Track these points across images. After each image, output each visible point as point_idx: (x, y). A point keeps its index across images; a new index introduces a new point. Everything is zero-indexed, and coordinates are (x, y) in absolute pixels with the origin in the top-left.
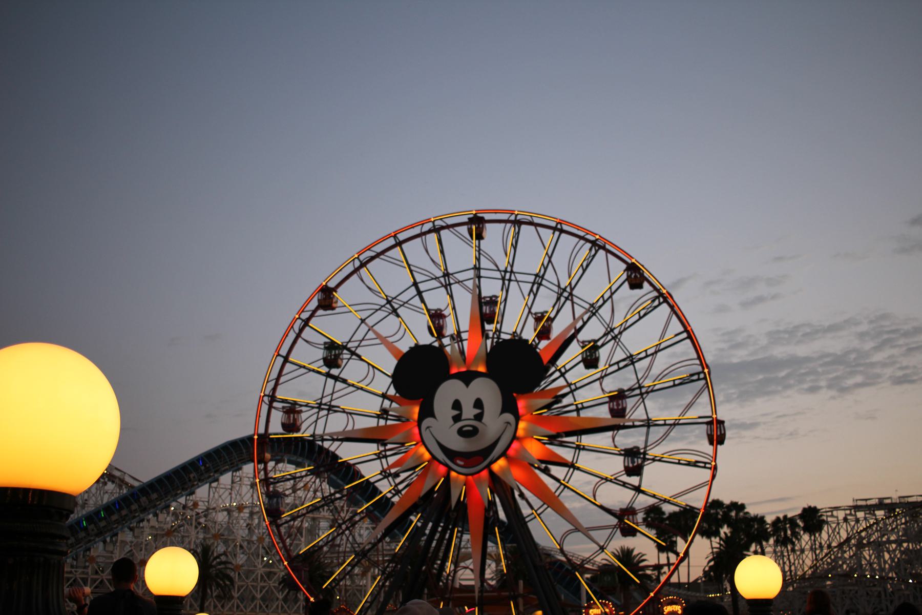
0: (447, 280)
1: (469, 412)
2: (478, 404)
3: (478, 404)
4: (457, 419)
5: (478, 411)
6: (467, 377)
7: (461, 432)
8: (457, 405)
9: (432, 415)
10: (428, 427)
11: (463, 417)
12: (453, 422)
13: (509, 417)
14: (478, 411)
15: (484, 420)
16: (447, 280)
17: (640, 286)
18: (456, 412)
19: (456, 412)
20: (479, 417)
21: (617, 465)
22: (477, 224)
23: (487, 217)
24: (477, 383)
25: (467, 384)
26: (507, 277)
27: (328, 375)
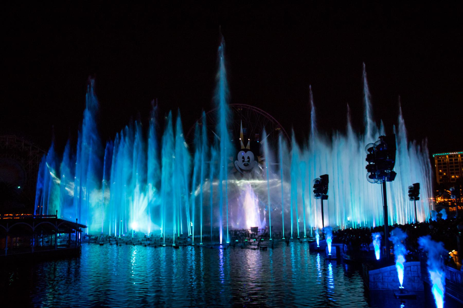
1: (246, 160)
2: (249, 158)
3: (249, 158)
4: (243, 161)
5: (248, 160)
6: (246, 151)
7: (245, 165)
8: (243, 158)
9: (237, 160)
10: (236, 163)
11: (245, 161)
12: (242, 162)
14: (248, 160)
15: (250, 162)
18: (243, 160)
19: (243, 160)
20: (249, 161)
25: (246, 153)
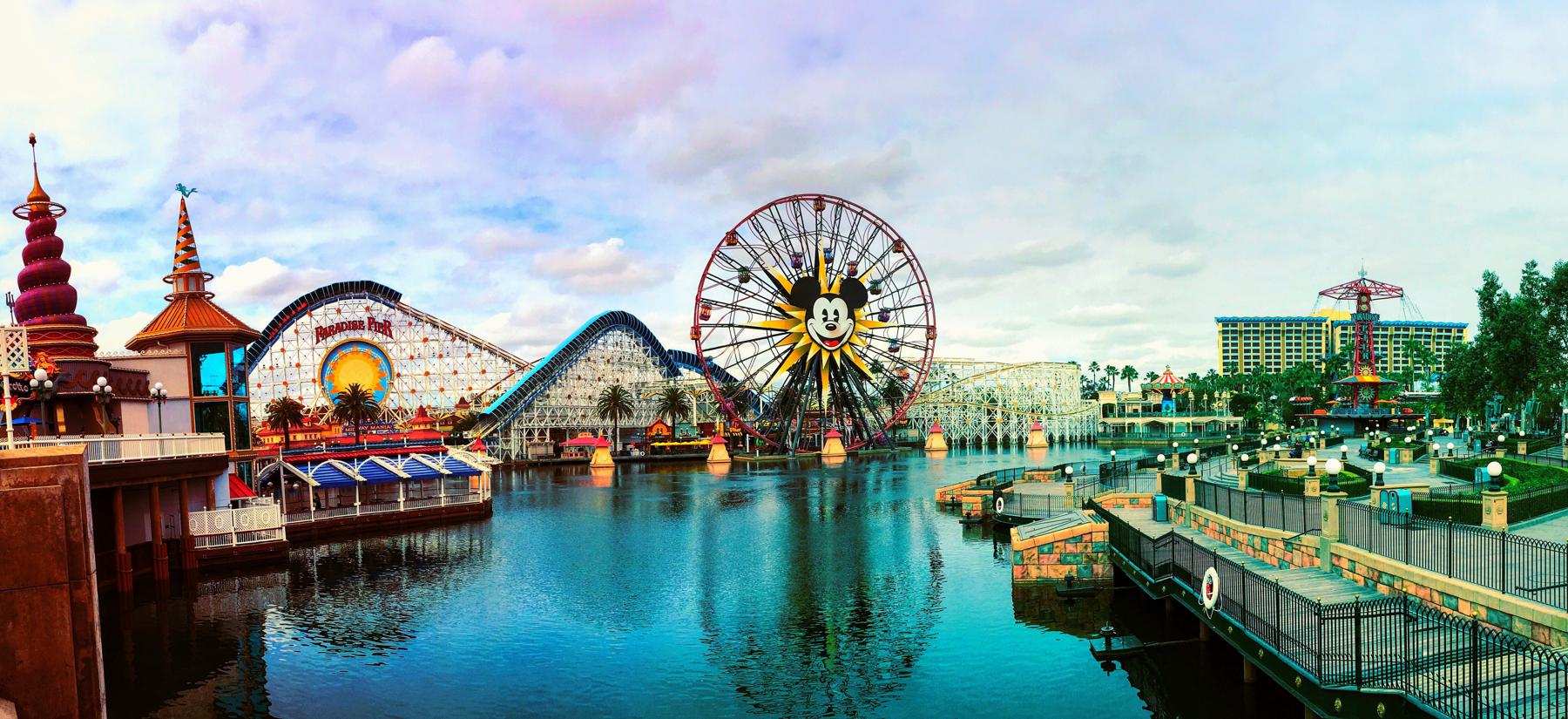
0: (802, 235)
1: (831, 317)
2: (836, 312)
3: (836, 312)
4: (825, 320)
6: (830, 297)
7: (827, 327)
8: (825, 312)
13: (851, 321)
16: (802, 235)
17: (899, 252)
20: (836, 320)
21: (885, 346)
22: (819, 202)
23: (825, 198)
24: (836, 300)
26: (835, 237)
27: (737, 289)
